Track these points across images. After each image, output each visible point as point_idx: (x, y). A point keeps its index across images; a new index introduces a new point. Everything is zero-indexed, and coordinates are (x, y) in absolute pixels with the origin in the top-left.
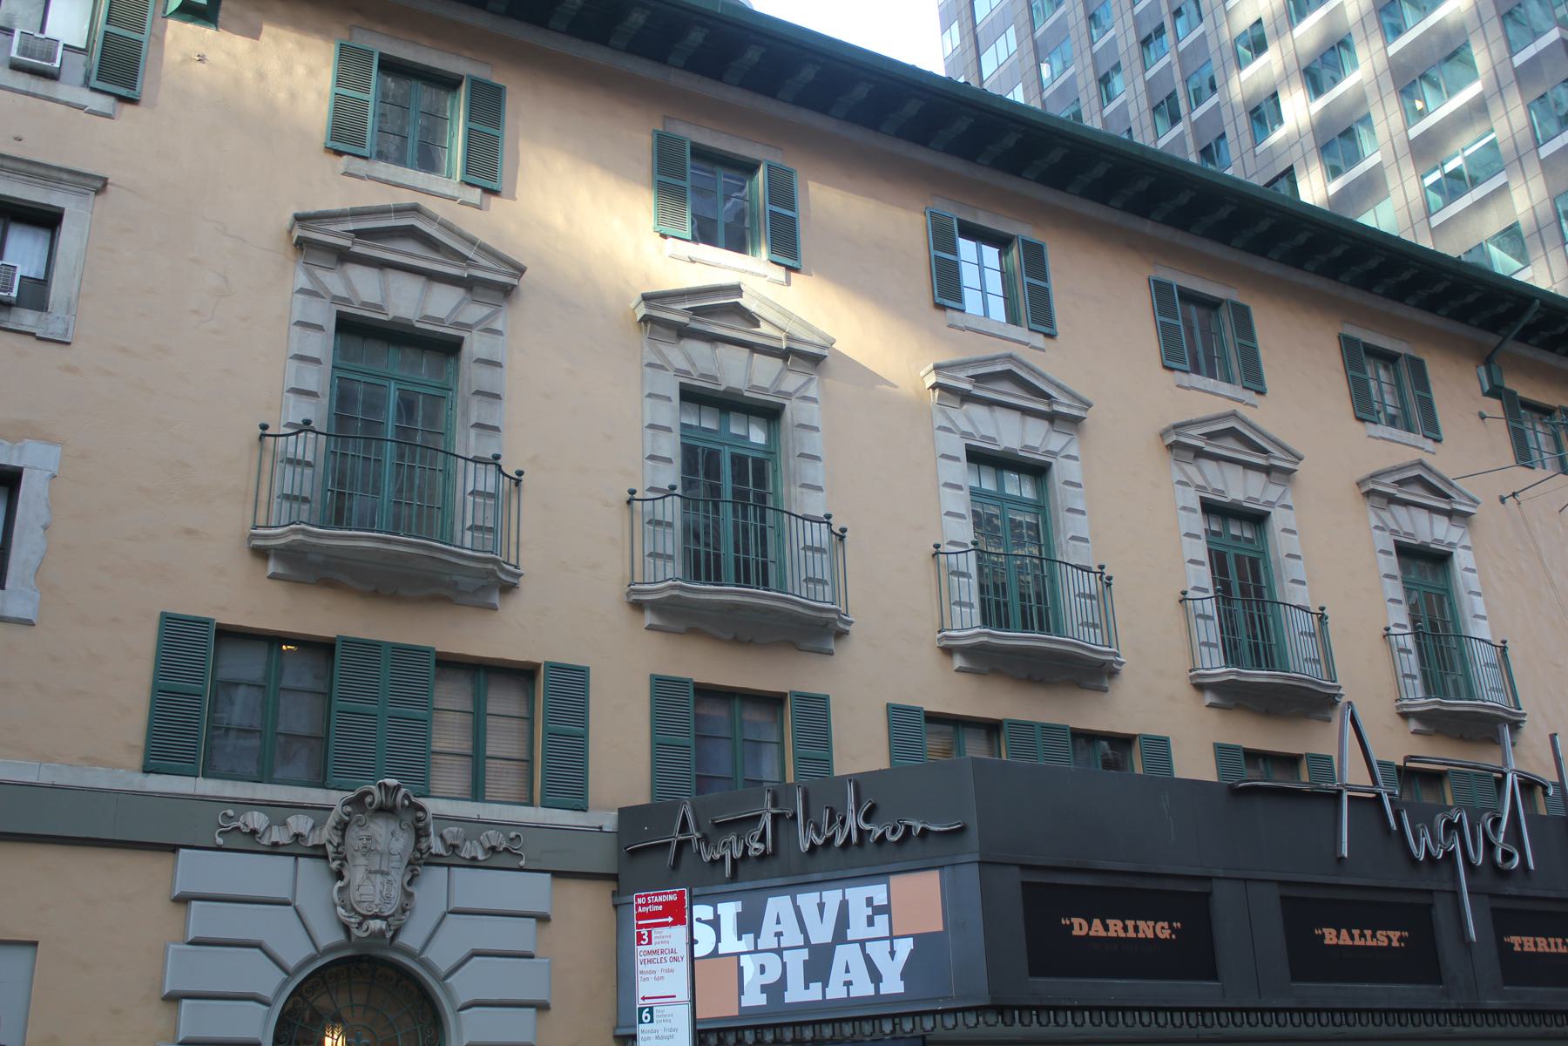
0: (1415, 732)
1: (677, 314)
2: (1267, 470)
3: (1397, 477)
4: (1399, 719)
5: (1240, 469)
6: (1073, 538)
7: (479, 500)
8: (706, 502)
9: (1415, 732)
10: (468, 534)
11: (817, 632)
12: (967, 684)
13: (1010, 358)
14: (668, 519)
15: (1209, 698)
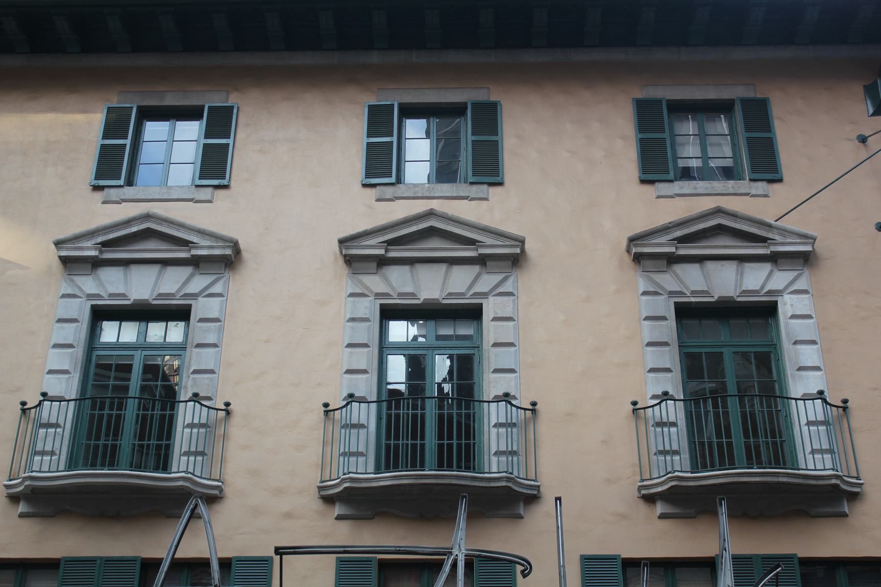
0: (662, 516)
1: (372, 248)
2: (482, 261)
3: (679, 233)
4: (642, 506)
5: (443, 267)
6: (196, 372)
7: (502, 430)
8: (452, 399)
9: (662, 516)
10: (494, 459)
11: (509, 500)
12: (30, 527)
13: (147, 217)
14: (672, 419)
15: (338, 510)
